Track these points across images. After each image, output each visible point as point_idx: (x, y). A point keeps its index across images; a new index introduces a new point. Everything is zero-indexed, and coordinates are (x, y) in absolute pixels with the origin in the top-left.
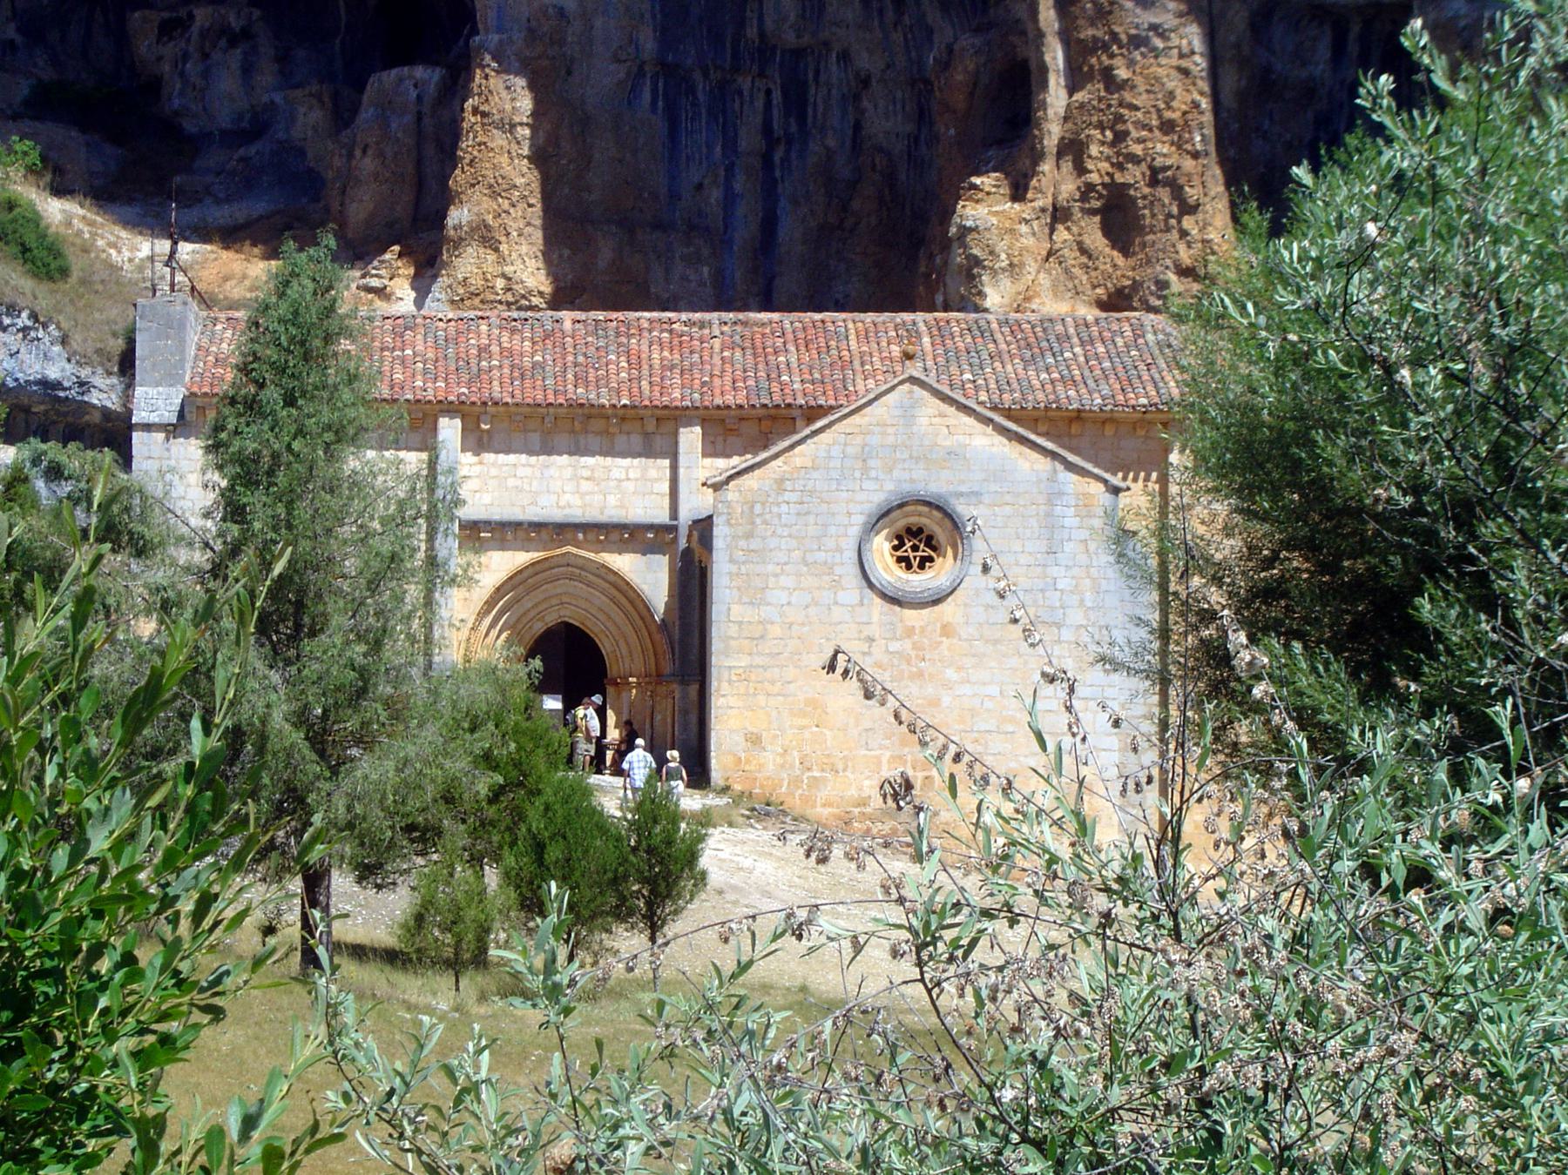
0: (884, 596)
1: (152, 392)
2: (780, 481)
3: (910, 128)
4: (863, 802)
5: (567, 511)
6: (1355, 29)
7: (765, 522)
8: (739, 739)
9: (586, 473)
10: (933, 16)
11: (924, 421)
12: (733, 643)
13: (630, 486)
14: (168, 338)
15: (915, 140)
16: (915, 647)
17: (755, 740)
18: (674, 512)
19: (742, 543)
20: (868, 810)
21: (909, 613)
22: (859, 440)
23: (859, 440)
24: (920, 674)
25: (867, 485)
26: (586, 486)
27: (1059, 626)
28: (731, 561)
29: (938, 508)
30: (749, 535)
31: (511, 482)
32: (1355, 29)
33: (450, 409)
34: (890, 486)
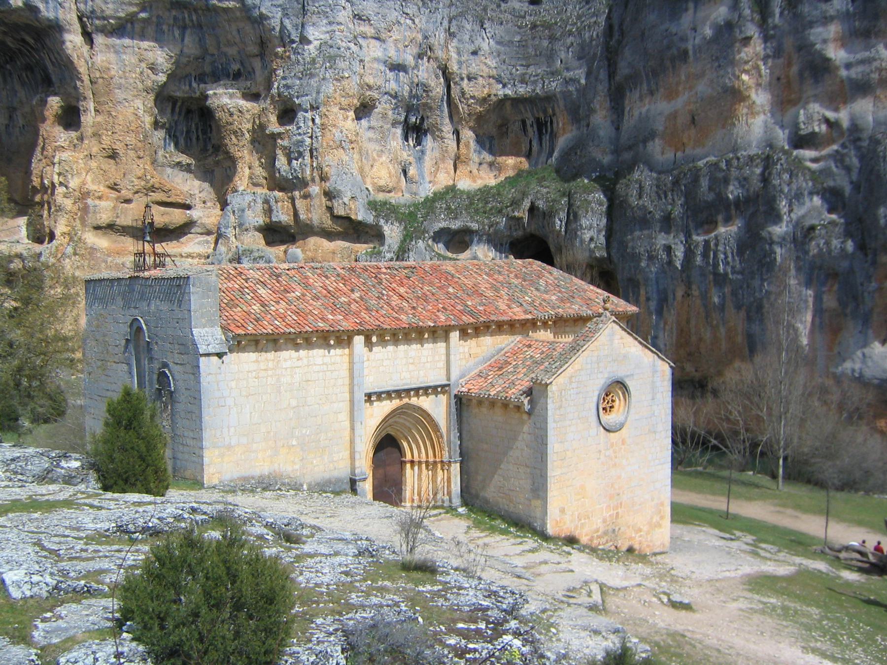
0: (604, 428)
1: (203, 331)
2: (571, 377)
3: (7, 122)
4: (597, 530)
5: (404, 382)
6: (179, 104)
7: (566, 400)
8: (557, 511)
9: (411, 361)
10: (18, 87)
11: (616, 341)
12: (555, 463)
13: (428, 365)
14: (208, 297)
15: (7, 126)
16: (615, 452)
17: (562, 511)
18: (449, 379)
19: (558, 412)
20: (599, 534)
21: (612, 434)
22: (596, 354)
23: (596, 354)
24: (615, 465)
25: (600, 376)
26: (411, 367)
27: (655, 432)
28: (554, 421)
29: (621, 383)
30: (560, 407)
31: (381, 369)
32: (179, 104)
33: (359, 333)
34: (606, 376)
